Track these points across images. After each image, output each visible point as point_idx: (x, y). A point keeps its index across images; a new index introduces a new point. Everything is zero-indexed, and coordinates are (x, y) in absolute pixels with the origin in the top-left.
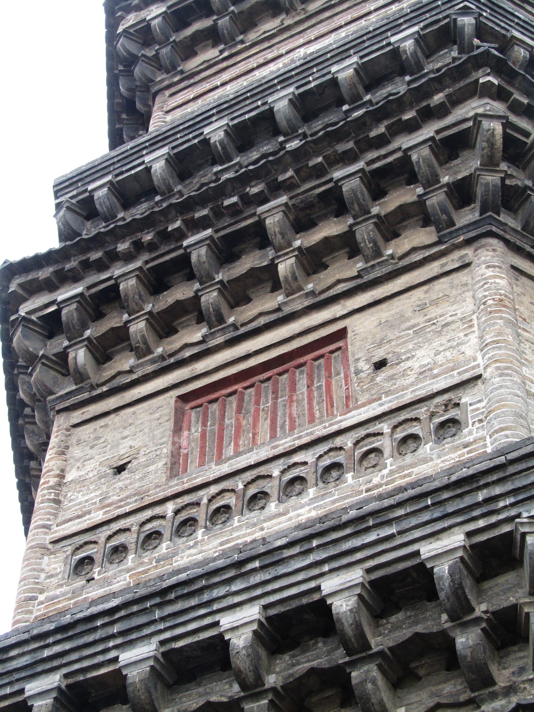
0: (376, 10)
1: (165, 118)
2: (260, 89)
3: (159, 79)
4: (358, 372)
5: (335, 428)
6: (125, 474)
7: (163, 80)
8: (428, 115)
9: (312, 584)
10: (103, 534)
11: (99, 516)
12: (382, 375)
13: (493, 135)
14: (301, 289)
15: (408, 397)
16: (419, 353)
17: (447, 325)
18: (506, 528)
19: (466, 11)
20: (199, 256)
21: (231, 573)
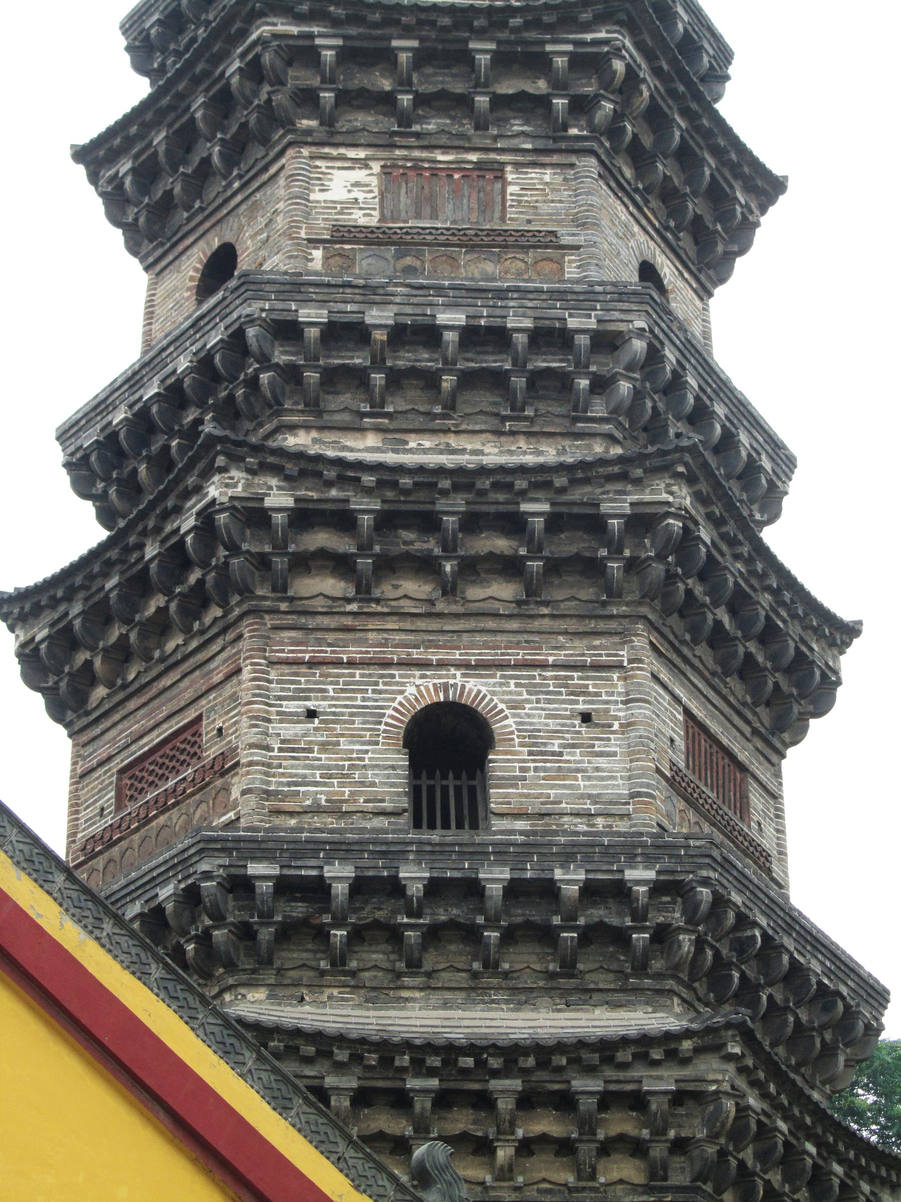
0: (556, 666)
1: (268, 673)
2: (471, 850)
3: (259, 592)
7: (264, 598)
8: (673, 1056)
13: (727, 1117)
14: (511, 1179)
19: (706, 882)
20: (423, 1108)
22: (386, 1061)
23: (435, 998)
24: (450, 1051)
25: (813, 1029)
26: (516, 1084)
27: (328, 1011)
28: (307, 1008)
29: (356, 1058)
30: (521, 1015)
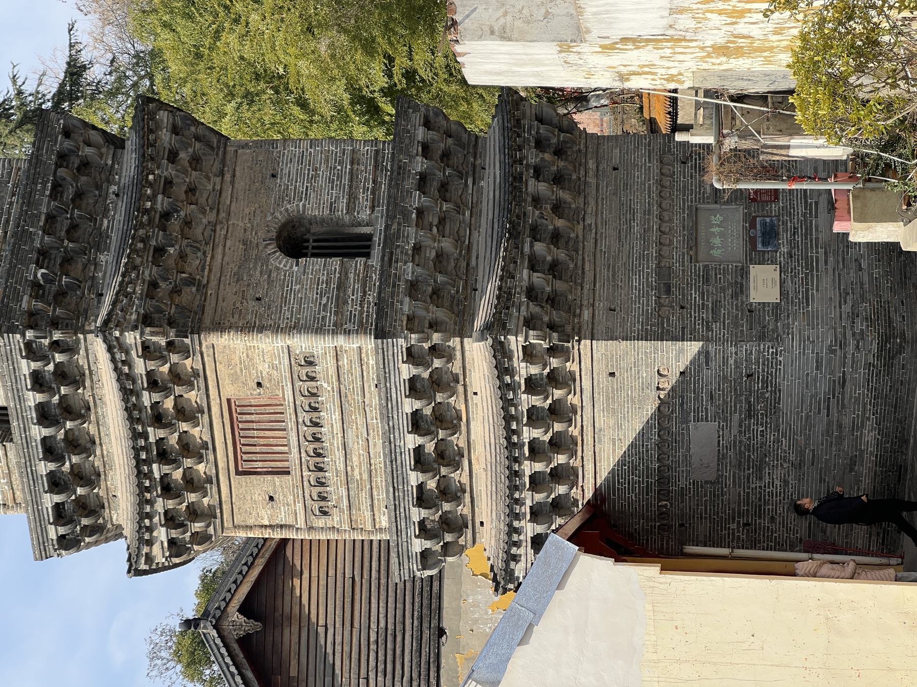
4: (260, 394)
5: (292, 405)
6: (276, 497)
9: (405, 416)
10: (309, 502)
11: (300, 506)
12: (266, 383)
15: (288, 375)
16: (260, 368)
17: (247, 356)
18: (404, 350)
21: (393, 445)
22: (148, 489)
23: (105, 440)
24: (139, 462)
25: (77, 186)
26: (150, 430)
27: (119, 485)
28: (119, 494)
29: (148, 502)
30: (108, 402)
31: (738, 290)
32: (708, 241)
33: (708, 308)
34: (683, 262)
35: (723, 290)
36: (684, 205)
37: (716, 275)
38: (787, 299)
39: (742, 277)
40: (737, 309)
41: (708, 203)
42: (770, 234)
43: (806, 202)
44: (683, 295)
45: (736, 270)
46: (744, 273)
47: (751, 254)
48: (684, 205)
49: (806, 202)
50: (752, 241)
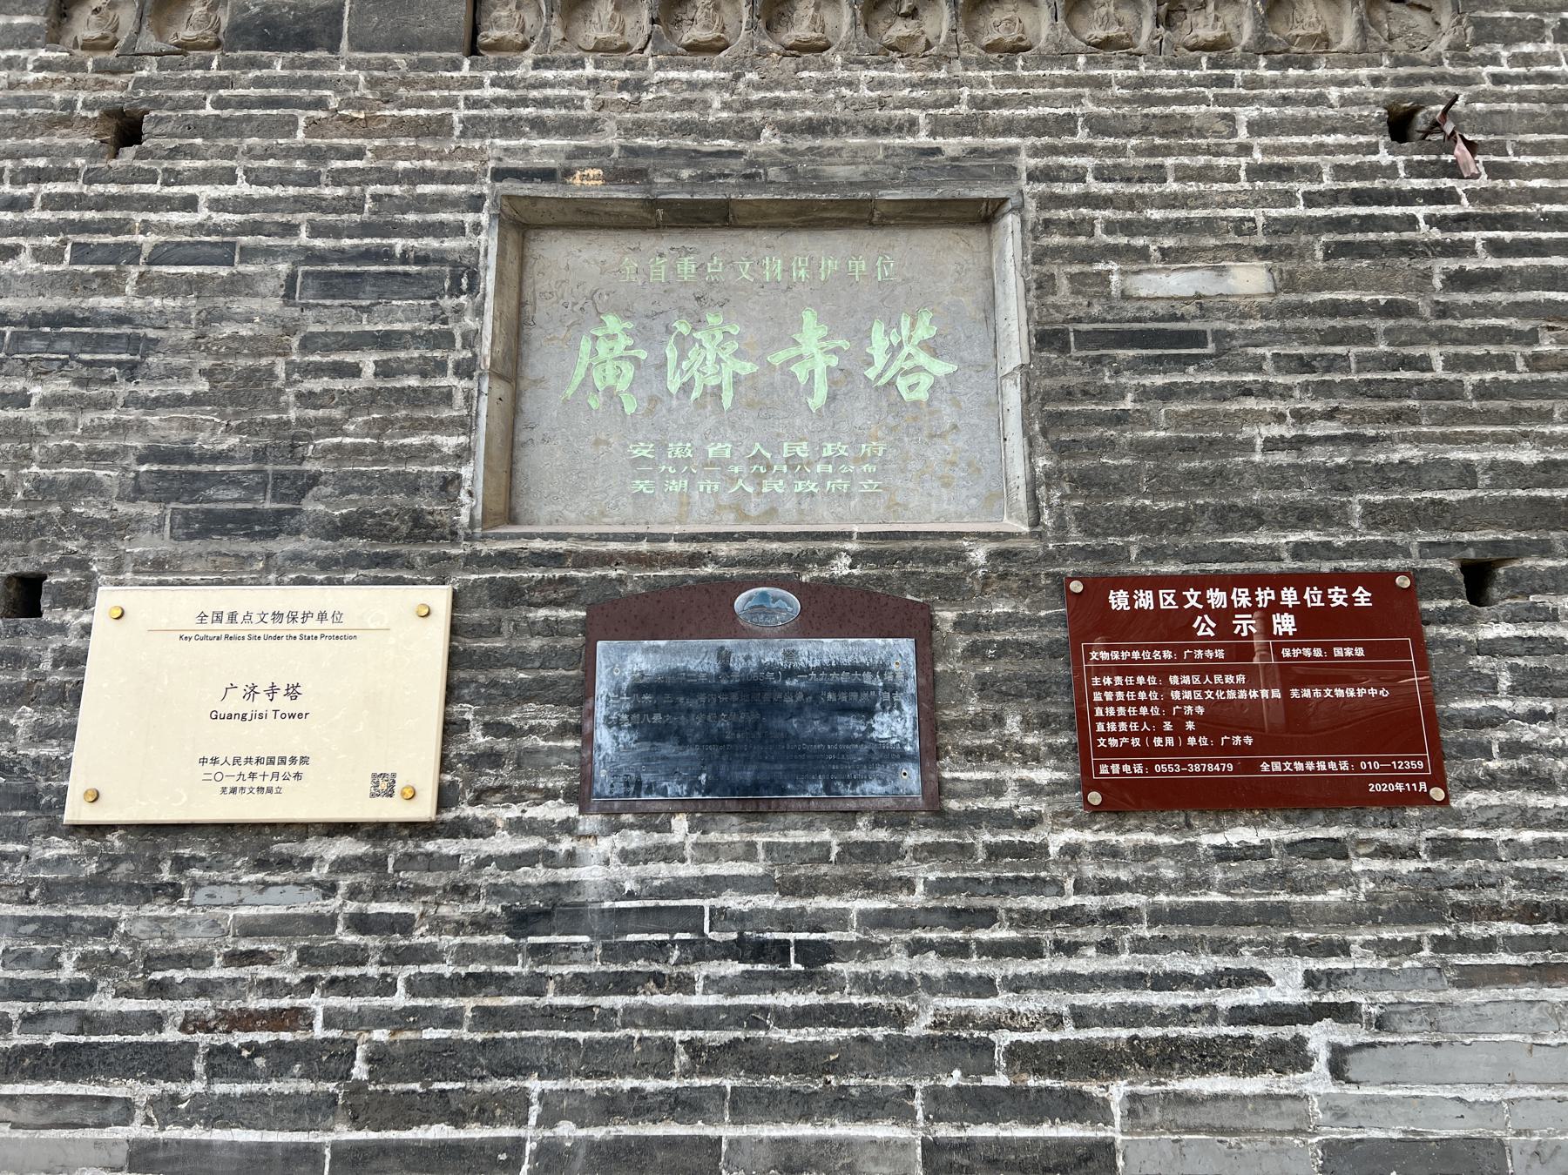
31: (226, 499)
32: (702, 301)
33: (78, 284)
34: (509, 127)
35: (242, 391)
36: (1009, 128)
37: (384, 341)
38: (95, 888)
39: (348, 527)
40: (44, 489)
41: (1043, 286)
42: (749, 744)
43: (1102, 1061)
44: (220, 127)
45: (412, 486)
46: (385, 541)
47: (566, 593)
48: (1009, 128)
49: (1102, 1061)
50: (683, 597)
